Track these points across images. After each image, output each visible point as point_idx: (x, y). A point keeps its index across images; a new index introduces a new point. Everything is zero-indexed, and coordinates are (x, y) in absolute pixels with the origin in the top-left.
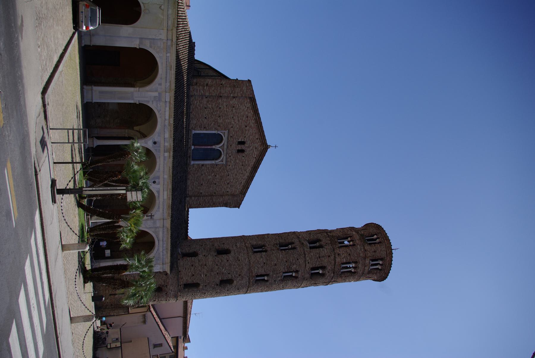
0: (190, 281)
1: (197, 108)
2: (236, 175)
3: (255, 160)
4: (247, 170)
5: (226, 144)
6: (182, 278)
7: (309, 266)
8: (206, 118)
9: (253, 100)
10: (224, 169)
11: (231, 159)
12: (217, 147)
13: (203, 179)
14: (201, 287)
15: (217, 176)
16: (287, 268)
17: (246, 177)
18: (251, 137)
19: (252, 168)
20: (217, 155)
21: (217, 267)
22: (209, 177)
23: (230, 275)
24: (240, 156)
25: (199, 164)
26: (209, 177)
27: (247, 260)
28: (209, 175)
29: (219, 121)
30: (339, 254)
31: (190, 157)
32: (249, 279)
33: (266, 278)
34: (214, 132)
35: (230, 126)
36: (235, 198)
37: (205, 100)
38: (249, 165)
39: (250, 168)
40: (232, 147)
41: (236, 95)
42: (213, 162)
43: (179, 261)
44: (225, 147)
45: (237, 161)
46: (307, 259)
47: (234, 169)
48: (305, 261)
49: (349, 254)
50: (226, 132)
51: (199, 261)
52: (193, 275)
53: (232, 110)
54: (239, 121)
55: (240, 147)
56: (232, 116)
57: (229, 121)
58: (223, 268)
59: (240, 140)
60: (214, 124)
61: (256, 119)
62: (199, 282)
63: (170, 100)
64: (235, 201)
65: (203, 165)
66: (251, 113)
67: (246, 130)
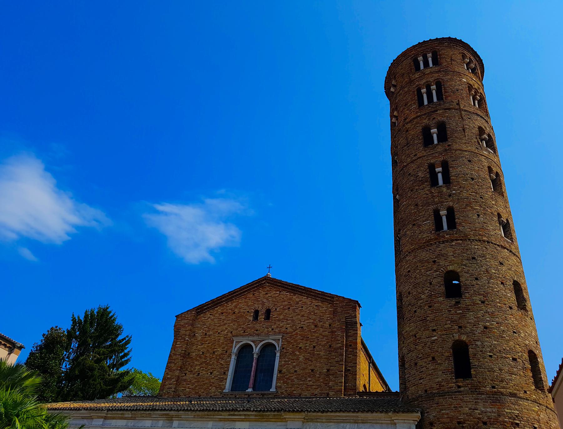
0: (448, 364)
1: (196, 386)
2: (303, 316)
3: (284, 293)
4: (298, 300)
5: (251, 338)
6: (439, 383)
7: (422, 152)
8: (211, 373)
9: (200, 310)
10: (291, 337)
11: (277, 327)
12: (256, 350)
13: (304, 369)
14: (464, 338)
15: (300, 346)
16: (423, 184)
17: (308, 301)
18: (250, 303)
19: (295, 294)
20: (268, 348)
21: (419, 311)
22: (301, 358)
23: (434, 282)
24: (274, 315)
25: (278, 379)
26: (301, 358)
27: (407, 258)
28: (298, 359)
29: (219, 353)
30: (405, 119)
31: (263, 395)
32: (443, 242)
33: (443, 213)
34: (233, 357)
35: (230, 335)
36: (339, 310)
37: (189, 376)
38: (290, 299)
39: (294, 297)
40: (258, 328)
41: (188, 333)
42: (278, 354)
43: (410, 398)
44: (255, 338)
45: (282, 317)
46: (409, 160)
47: (293, 321)
48: (412, 162)
49: (405, 105)
50: (235, 339)
51: (410, 351)
52: (433, 358)
53: (209, 335)
54: (225, 324)
55: (261, 317)
56: (217, 335)
57: (222, 338)
58: (419, 299)
59: (251, 319)
60: (223, 359)
61: (227, 301)
62: (450, 344)
63: (102, 417)
64: (345, 311)
65: (280, 371)
66: (219, 309)
67: (239, 313)
